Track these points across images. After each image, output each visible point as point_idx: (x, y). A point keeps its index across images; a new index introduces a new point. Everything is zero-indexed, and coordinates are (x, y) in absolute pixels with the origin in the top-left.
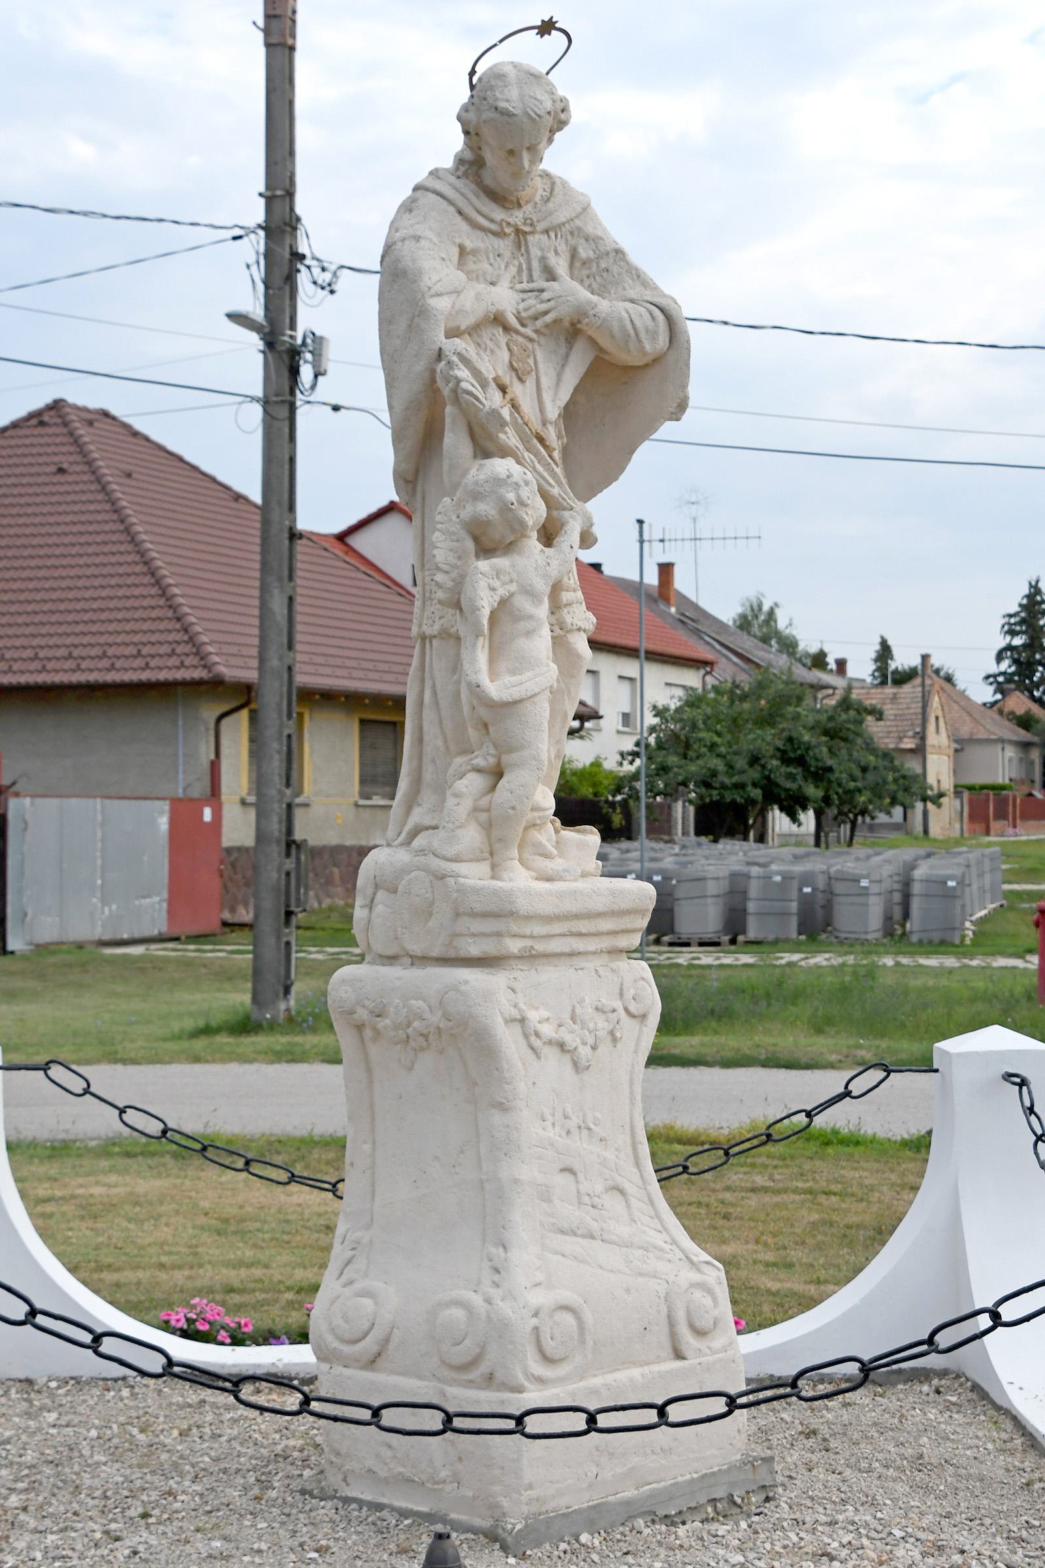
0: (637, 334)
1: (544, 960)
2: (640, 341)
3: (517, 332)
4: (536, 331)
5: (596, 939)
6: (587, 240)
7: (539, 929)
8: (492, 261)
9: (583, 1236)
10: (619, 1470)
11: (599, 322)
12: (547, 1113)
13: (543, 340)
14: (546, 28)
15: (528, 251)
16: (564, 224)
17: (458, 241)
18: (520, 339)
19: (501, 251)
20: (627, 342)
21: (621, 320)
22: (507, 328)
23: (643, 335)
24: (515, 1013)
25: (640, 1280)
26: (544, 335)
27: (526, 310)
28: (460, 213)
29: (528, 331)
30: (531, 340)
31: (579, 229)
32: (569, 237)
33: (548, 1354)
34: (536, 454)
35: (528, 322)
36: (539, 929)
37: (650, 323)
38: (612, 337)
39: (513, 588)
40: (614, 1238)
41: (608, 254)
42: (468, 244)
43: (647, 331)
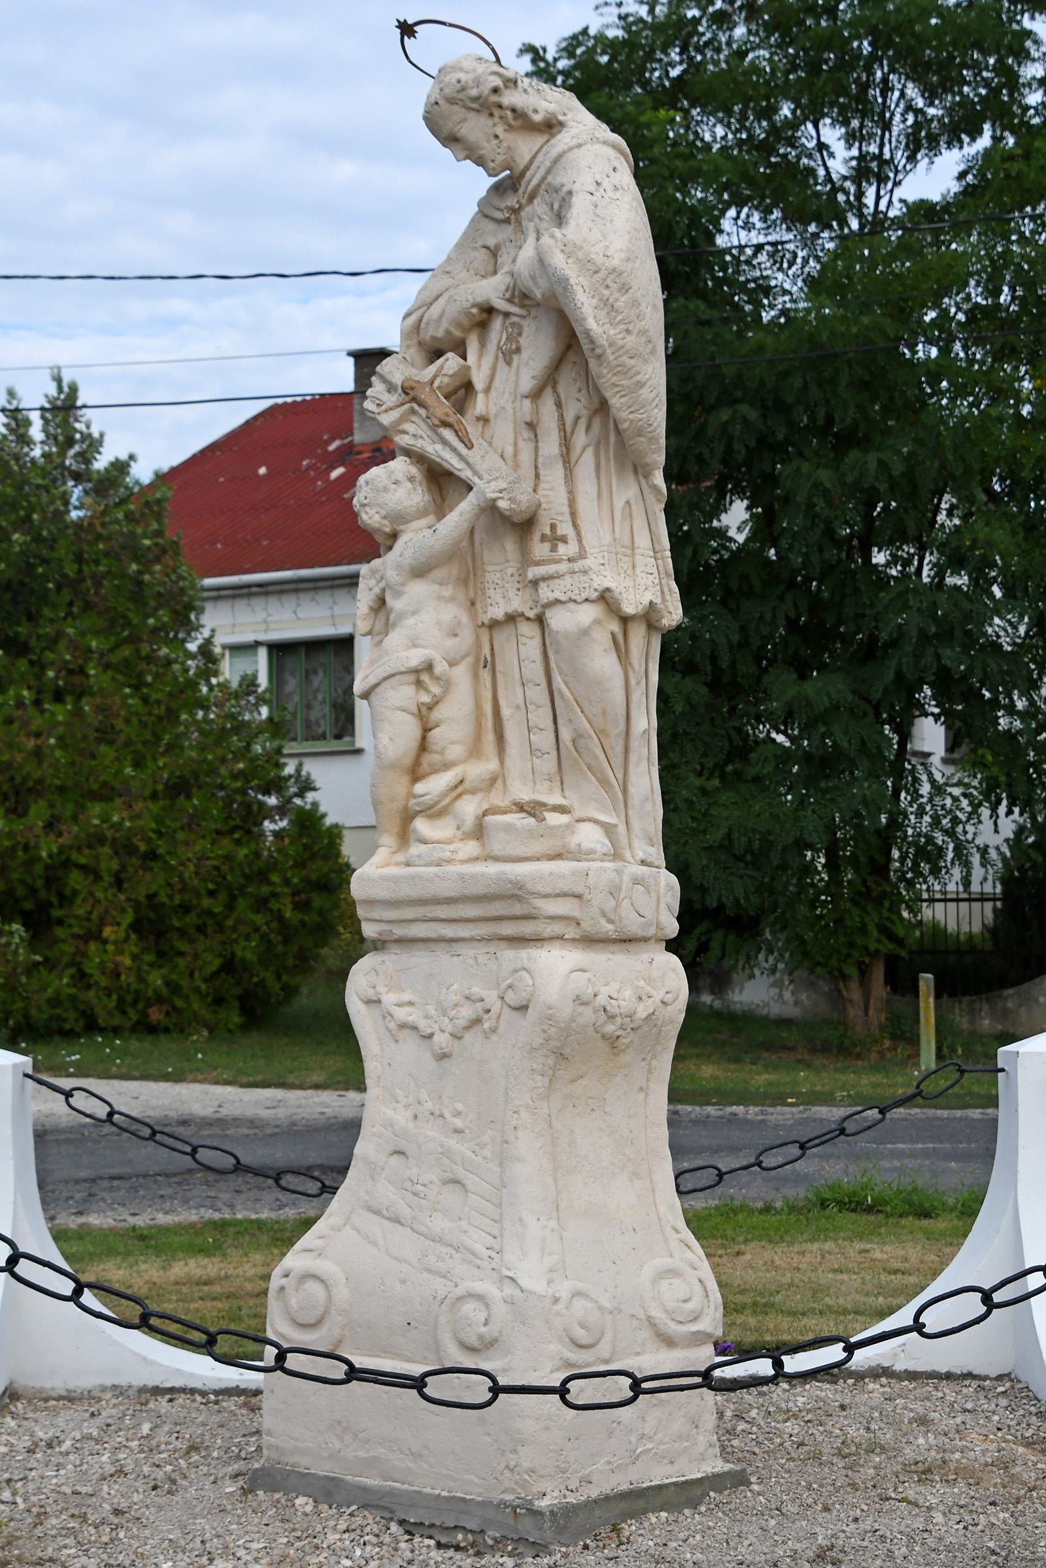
1: (421, 945)
5: (471, 925)
7: (388, 914)
9: (389, 1219)
10: (361, 1454)
12: (399, 1093)
14: (407, 30)
16: (539, 185)
17: (480, 243)
24: (371, 994)
25: (426, 1275)
30: (523, 317)
33: (312, 1321)
34: (445, 442)
36: (388, 914)
39: (382, 585)
40: (423, 1229)
42: (491, 242)
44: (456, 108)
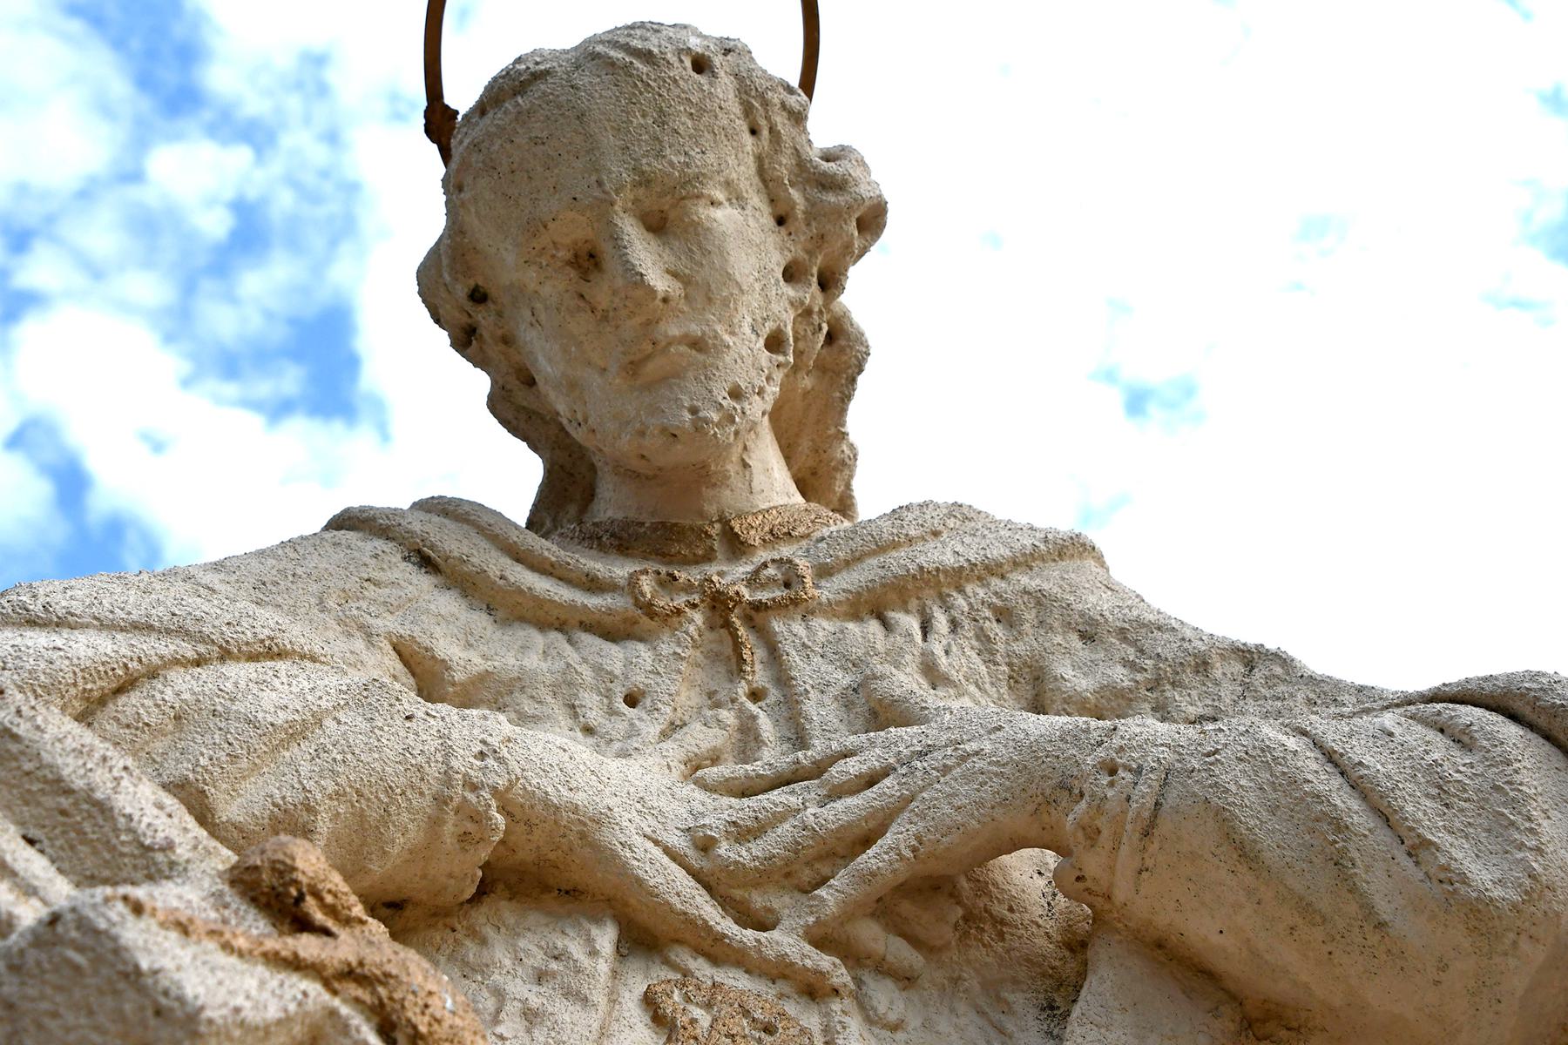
0: (1385, 816)
2: (1418, 848)
3: (717, 951)
4: (821, 940)
6: (1087, 637)
8: (595, 716)
11: (1145, 792)
13: (884, 996)
15: (783, 679)
18: (737, 981)
19: (639, 679)
20: (1338, 862)
21: (1285, 789)
22: (645, 935)
23: (1419, 809)
26: (883, 969)
27: (743, 833)
28: (426, 561)
29: (786, 942)
30: (814, 990)
31: (1040, 600)
32: (997, 630)
35: (780, 902)
37: (1456, 764)
38: (1245, 853)
41: (1202, 665)
43: (1442, 790)
44: (748, 139)
